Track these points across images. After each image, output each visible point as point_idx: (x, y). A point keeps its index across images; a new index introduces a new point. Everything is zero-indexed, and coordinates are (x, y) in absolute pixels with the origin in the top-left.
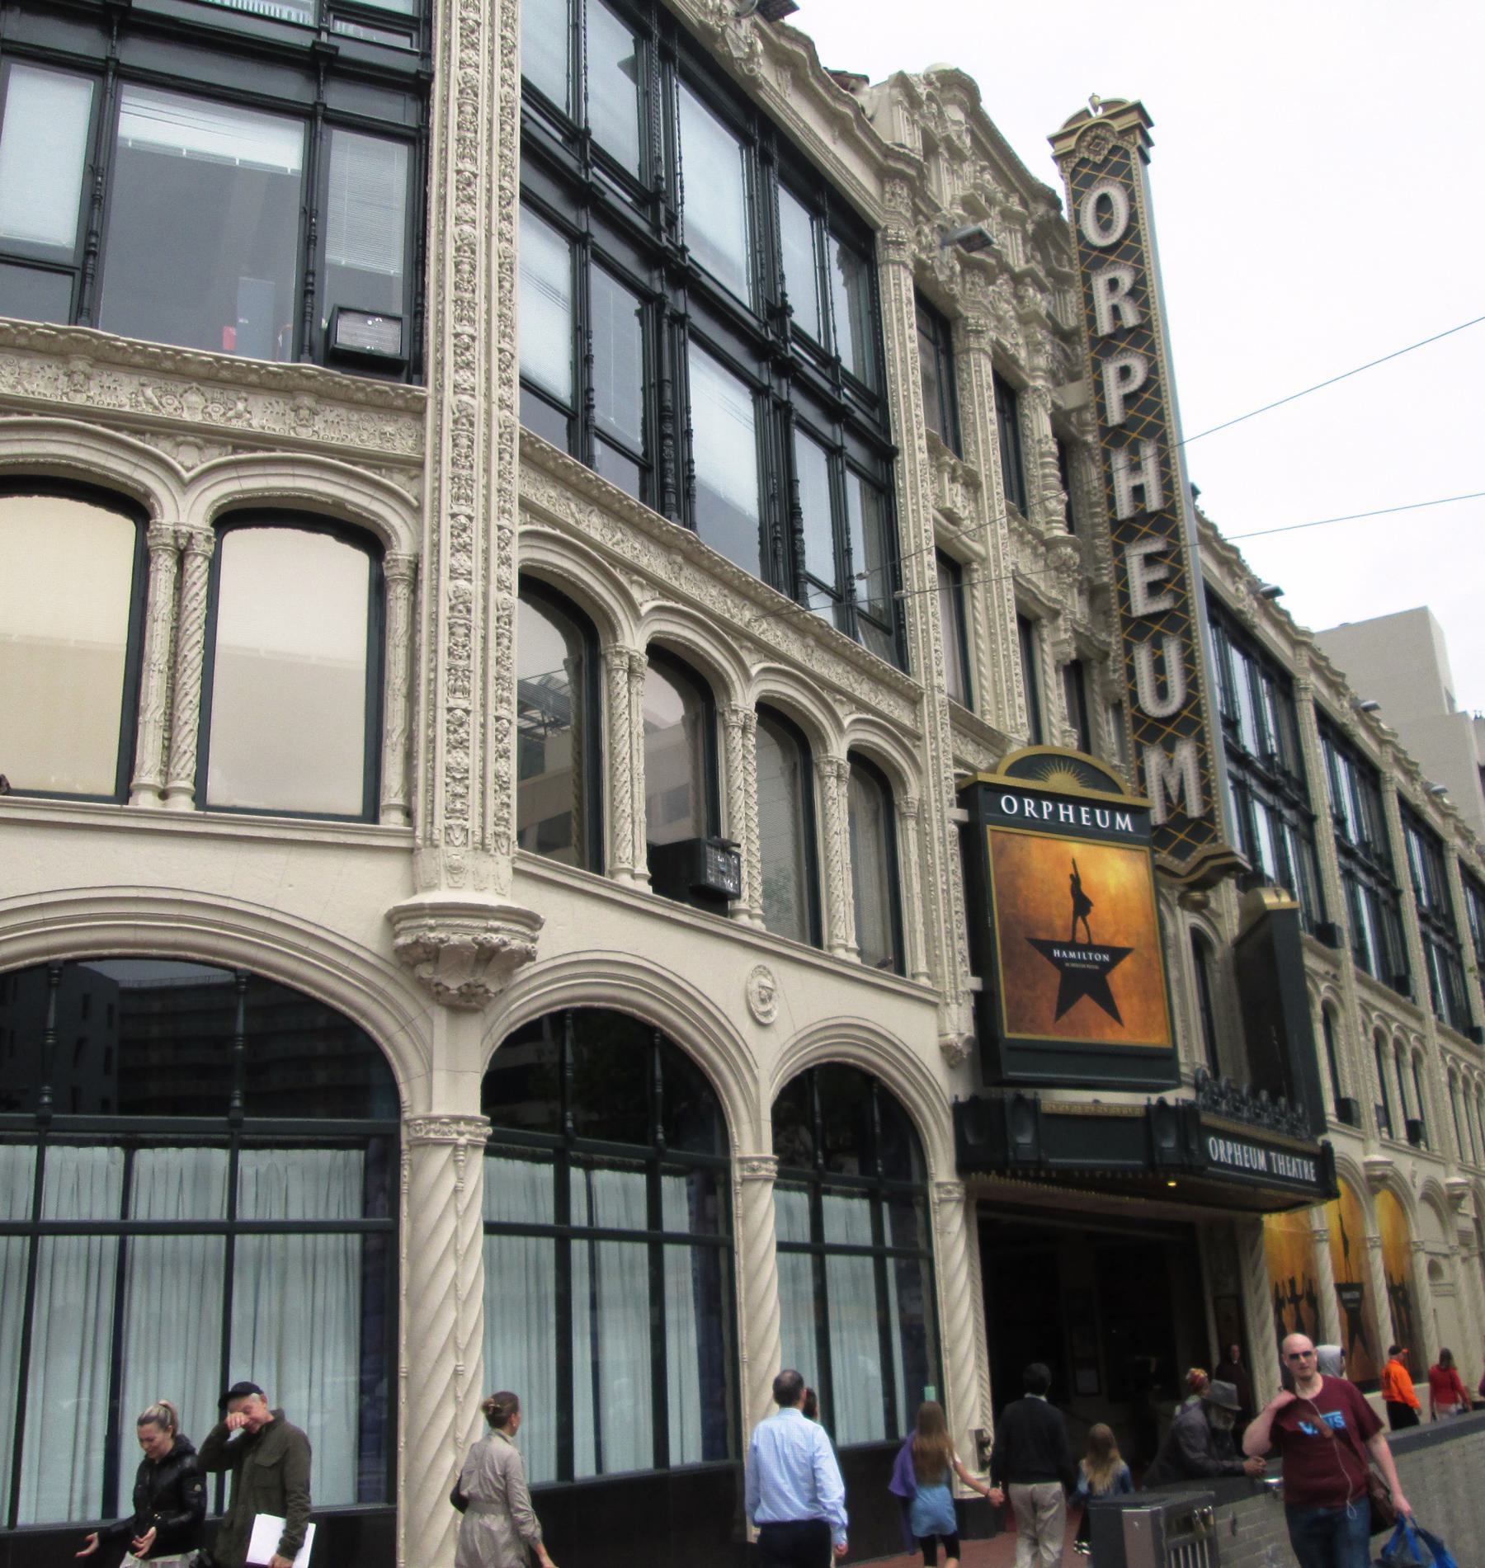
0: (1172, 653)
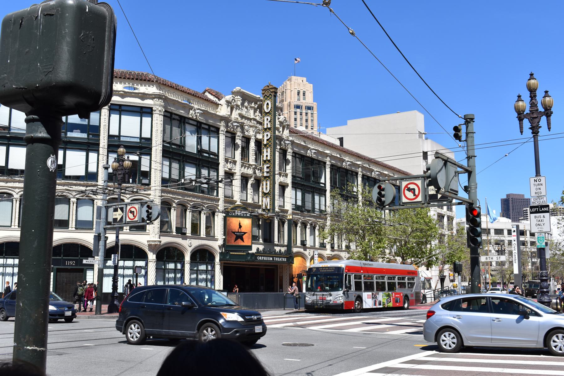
0: (268, 183)
